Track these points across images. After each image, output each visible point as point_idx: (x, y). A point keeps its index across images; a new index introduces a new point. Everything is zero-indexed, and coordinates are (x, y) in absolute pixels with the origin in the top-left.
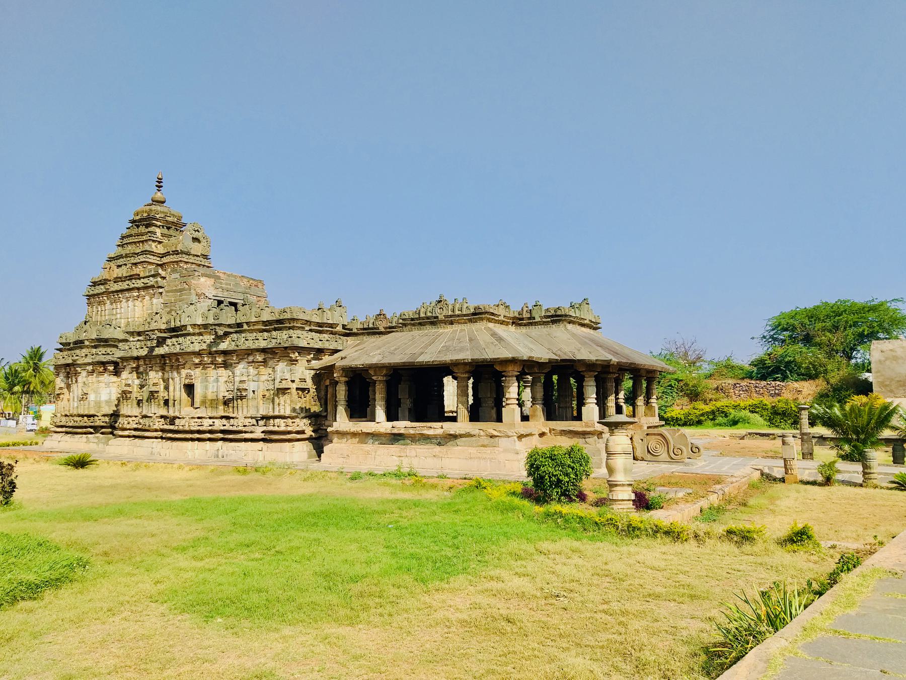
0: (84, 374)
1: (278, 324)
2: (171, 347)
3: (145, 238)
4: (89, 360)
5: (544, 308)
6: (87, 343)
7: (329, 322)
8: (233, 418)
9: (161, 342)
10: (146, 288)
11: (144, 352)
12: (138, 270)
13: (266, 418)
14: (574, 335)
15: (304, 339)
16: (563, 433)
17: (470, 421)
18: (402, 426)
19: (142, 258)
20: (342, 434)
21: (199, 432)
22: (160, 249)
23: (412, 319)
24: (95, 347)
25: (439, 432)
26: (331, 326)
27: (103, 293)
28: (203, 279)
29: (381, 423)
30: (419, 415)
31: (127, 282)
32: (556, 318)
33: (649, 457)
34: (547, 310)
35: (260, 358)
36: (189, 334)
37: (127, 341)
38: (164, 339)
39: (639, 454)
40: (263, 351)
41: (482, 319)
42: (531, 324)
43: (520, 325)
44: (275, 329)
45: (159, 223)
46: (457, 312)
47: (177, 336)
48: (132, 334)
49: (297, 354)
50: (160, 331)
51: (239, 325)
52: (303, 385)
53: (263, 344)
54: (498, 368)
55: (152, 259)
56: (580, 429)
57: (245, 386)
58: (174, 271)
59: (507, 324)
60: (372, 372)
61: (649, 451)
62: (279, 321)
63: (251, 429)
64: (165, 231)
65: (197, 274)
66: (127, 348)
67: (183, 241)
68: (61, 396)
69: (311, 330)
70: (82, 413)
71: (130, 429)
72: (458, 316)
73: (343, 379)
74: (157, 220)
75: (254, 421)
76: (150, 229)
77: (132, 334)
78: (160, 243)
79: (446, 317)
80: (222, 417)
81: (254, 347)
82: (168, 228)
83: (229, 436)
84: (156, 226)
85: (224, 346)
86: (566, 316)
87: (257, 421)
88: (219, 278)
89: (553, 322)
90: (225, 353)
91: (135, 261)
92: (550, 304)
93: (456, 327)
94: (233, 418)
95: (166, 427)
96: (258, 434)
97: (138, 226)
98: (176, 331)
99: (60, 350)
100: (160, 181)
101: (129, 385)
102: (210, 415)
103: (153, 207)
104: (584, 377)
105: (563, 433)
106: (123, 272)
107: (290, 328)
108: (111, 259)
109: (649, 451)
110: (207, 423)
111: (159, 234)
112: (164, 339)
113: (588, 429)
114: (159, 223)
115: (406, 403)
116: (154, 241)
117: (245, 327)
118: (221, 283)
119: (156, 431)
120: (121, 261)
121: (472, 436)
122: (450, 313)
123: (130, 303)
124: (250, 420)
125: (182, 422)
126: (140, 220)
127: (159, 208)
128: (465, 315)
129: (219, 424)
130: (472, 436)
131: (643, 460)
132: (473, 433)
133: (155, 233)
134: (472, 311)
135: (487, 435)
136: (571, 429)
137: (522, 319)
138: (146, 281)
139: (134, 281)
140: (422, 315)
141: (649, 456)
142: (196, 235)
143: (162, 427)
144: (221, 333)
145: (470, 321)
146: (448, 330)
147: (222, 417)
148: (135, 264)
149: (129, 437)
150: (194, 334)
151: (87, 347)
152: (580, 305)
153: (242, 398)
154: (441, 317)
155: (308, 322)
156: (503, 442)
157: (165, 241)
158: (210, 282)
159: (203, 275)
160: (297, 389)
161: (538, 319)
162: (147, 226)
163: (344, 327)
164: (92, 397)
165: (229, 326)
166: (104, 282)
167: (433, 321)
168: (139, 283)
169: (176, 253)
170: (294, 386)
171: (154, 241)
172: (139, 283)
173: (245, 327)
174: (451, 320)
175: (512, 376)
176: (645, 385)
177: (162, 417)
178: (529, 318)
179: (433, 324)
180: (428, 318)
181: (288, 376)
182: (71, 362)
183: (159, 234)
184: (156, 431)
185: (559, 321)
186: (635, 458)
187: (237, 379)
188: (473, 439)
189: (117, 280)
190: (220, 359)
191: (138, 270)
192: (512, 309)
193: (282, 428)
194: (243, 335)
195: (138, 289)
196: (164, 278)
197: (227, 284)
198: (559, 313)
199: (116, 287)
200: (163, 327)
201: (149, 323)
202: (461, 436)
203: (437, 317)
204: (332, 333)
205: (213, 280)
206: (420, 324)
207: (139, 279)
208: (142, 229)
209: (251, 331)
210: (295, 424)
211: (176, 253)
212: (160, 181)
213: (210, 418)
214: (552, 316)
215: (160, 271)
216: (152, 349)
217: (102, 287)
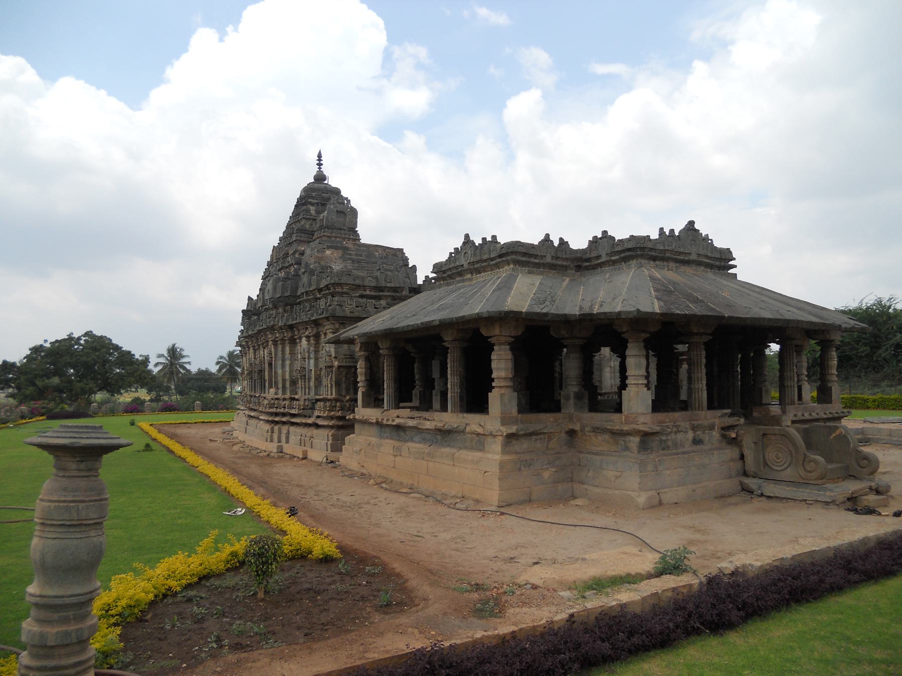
7: (388, 285)
26: (395, 289)
28: (328, 252)
43: (587, 268)
63: (307, 412)
69: (362, 296)
73: (362, 353)
84: (312, 204)
88: (347, 249)
104: (626, 341)
111: (313, 212)
113: (626, 428)
118: (350, 254)
133: (308, 211)
154: (466, 266)
158: (337, 254)
159: (328, 248)
161: (603, 259)
183: (313, 212)
185: (632, 258)
197: (357, 255)
205: (340, 252)
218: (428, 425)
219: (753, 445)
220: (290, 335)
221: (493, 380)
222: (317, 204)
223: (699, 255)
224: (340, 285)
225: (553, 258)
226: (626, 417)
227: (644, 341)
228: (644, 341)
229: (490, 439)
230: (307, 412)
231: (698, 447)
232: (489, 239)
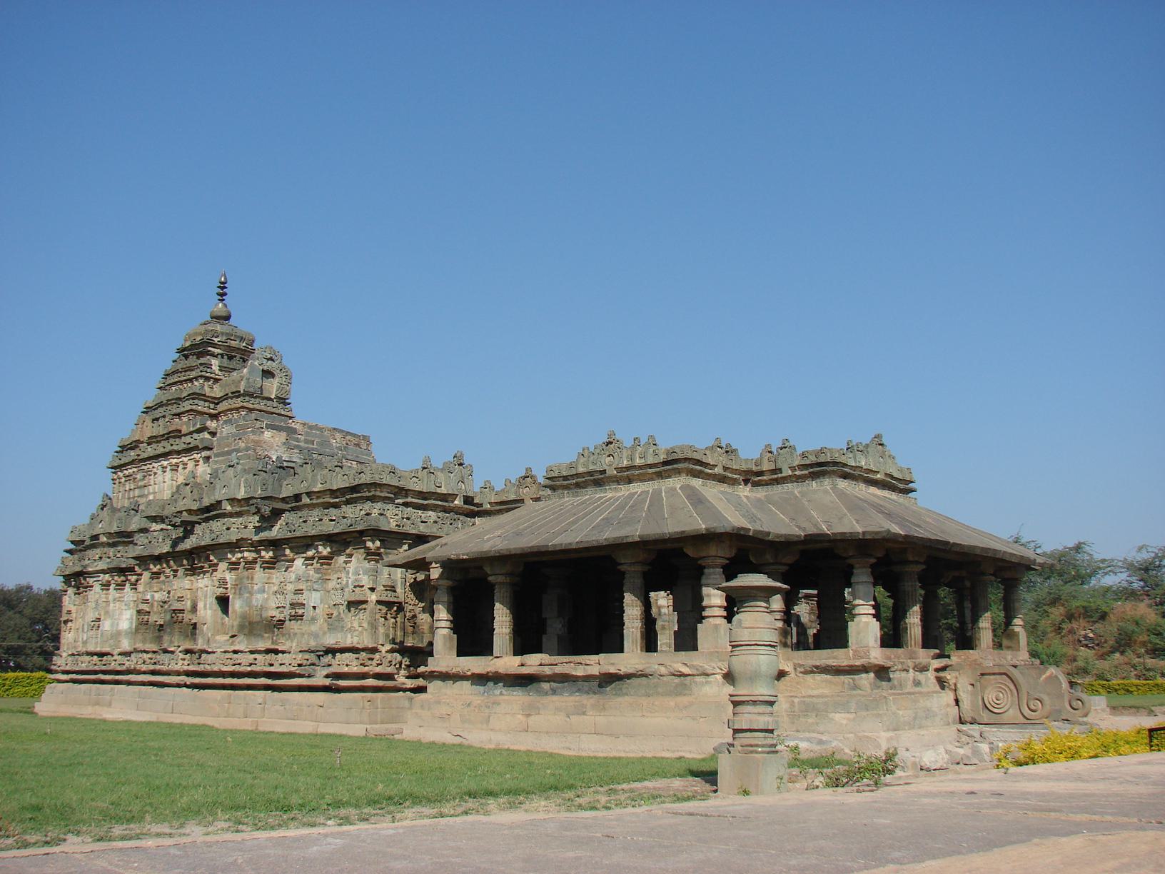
0: (97, 587)
1: (353, 494)
2: (202, 535)
3: (193, 374)
4: (102, 565)
5: (799, 451)
6: (103, 539)
7: (439, 490)
8: (283, 652)
9: (188, 528)
10: (189, 450)
11: (166, 549)
12: (184, 424)
13: (332, 651)
14: (842, 495)
15: (392, 517)
18: (533, 662)
19: (186, 406)
20: (445, 677)
21: (233, 675)
22: (217, 391)
23: (566, 478)
24: (113, 545)
25: (595, 670)
27: (132, 462)
28: (267, 434)
29: (505, 661)
30: (577, 645)
31: (164, 443)
32: (819, 468)
33: (985, 716)
34: (803, 455)
35: (325, 551)
36: (224, 515)
37: (144, 531)
38: (193, 524)
40: (329, 539)
41: (679, 472)
42: (777, 481)
44: (348, 502)
45: (217, 351)
46: (638, 461)
47: (207, 520)
48: (154, 519)
49: (378, 543)
50: (190, 512)
51: (297, 497)
52: (389, 597)
53: (329, 528)
54: (690, 551)
55: (202, 406)
57: (301, 598)
58: (228, 422)
59: (734, 482)
60: (488, 570)
62: (354, 489)
63: (310, 670)
64: (226, 362)
65: (258, 424)
66: (146, 541)
67: (245, 376)
68: (70, 624)
69: (406, 505)
70: (91, 648)
71: (144, 673)
72: (640, 467)
74: (215, 346)
75: (313, 658)
76: (202, 360)
77: (154, 519)
78: (217, 380)
79: (620, 470)
80: (268, 651)
81: (313, 533)
82: (230, 358)
83: (276, 682)
84: (213, 355)
85: (275, 533)
86: (835, 464)
87: (319, 656)
88: (294, 431)
89: (814, 476)
90: (275, 544)
91: (178, 411)
92: (808, 442)
93: (637, 488)
94: (283, 652)
95: (192, 668)
96: (319, 680)
97: (186, 357)
98: (211, 512)
99: (70, 552)
100: (223, 286)
101: (146, 601)
102: (251, 648)
103: (210, 327)
104: (852, 567)
106: (160, 429)
107: (368, 499)
108: (148, 410)
110: (246, 659)
111: (215, 368)
112: (193, 524)
114: (217, 351)
115: (555, 627)
116: (207, 379)
117: (306, 500)
118: (298, 440)
119: (178, 673)
120: (158, 413)
122: (625, 463)
123: (169, 474)
124: (307, 656)
125: (210, 658)
126: (193, 346)
127: (219, 327)
128: (651, 466)
129: (262, 663)
132: (648, 671)
133: (209, 366)
134: (662, 457)
137: (761, 473)
138: (188, 439)
139: (171, 441)
140: (581, 470)
142: (268, 365)
143: (186, 668)
144: (266, 510)
145: (660, 475)
146: (624, 490)
147: (268, 651)
148: (178, 415)
149: (143, 684)
150: (231, 515)
151: (103, 545)
152: (867, 446)
153: (297, 617)
154: (612, 472)
155: (401, 491)
157: (225, 378)
158: (281, 437)
159: (269, 427)
160: (379, 602)
161: (787, 472)
162: (200, 355)
163: (468, 500)
164: (106, 625)
165: (283, 500)
166: (135, 445)
167: (598, 479)
168: (179, 445)
169: (237, 394)
170: (373, 597)
171: (207, 379)
172: (179, 445)
173: (306, 500)
174: (628, 475)
175: (716, 566)
177: (187, 651)
178: (774, 471)
179: (598, 483)
180: (590, 473)
181: (366, 581)
182: (78, 569)
183: (215, 368)
184: (178, 673)
185: (823, 474)
187: (290, 587)
189: (153, 440)
190: (268, 555)
191: (184, 424)
192: (743, 454)
193: (355, 669)
194: (300, 514)
195: (178, 453)
196: (213, 434)
197: (306, 442)
198: (822, 459)
199: (150, 451)
200: (195, 507)
201: (176, 501)
202: (629, 676)
203: (604, 472)
204: (446, 510)
205: (284, 435)
206: (578, 485)
207: (180, 437)
208: (193, 361)
209: (311, 507)
210: (374, 662)
211: (237, 394)
212: (223, 286)
213: (252, 652)
214: (811, 466)
215: (209, 423)
216: (175, 543)
217: (132, 453)
218: (580, 672)
219: (970, 688)
220: (271, 554)
221: (704, 609)
222: (222, 355)
223: (886, 474)
224: (380, 485)
225: (726, 469)
226: (855, 651)
227: (872, 566)
228: (872, 566)
229: (702, 679)
230: (310, 670)
231: (917, 689)
232: (644, 440)
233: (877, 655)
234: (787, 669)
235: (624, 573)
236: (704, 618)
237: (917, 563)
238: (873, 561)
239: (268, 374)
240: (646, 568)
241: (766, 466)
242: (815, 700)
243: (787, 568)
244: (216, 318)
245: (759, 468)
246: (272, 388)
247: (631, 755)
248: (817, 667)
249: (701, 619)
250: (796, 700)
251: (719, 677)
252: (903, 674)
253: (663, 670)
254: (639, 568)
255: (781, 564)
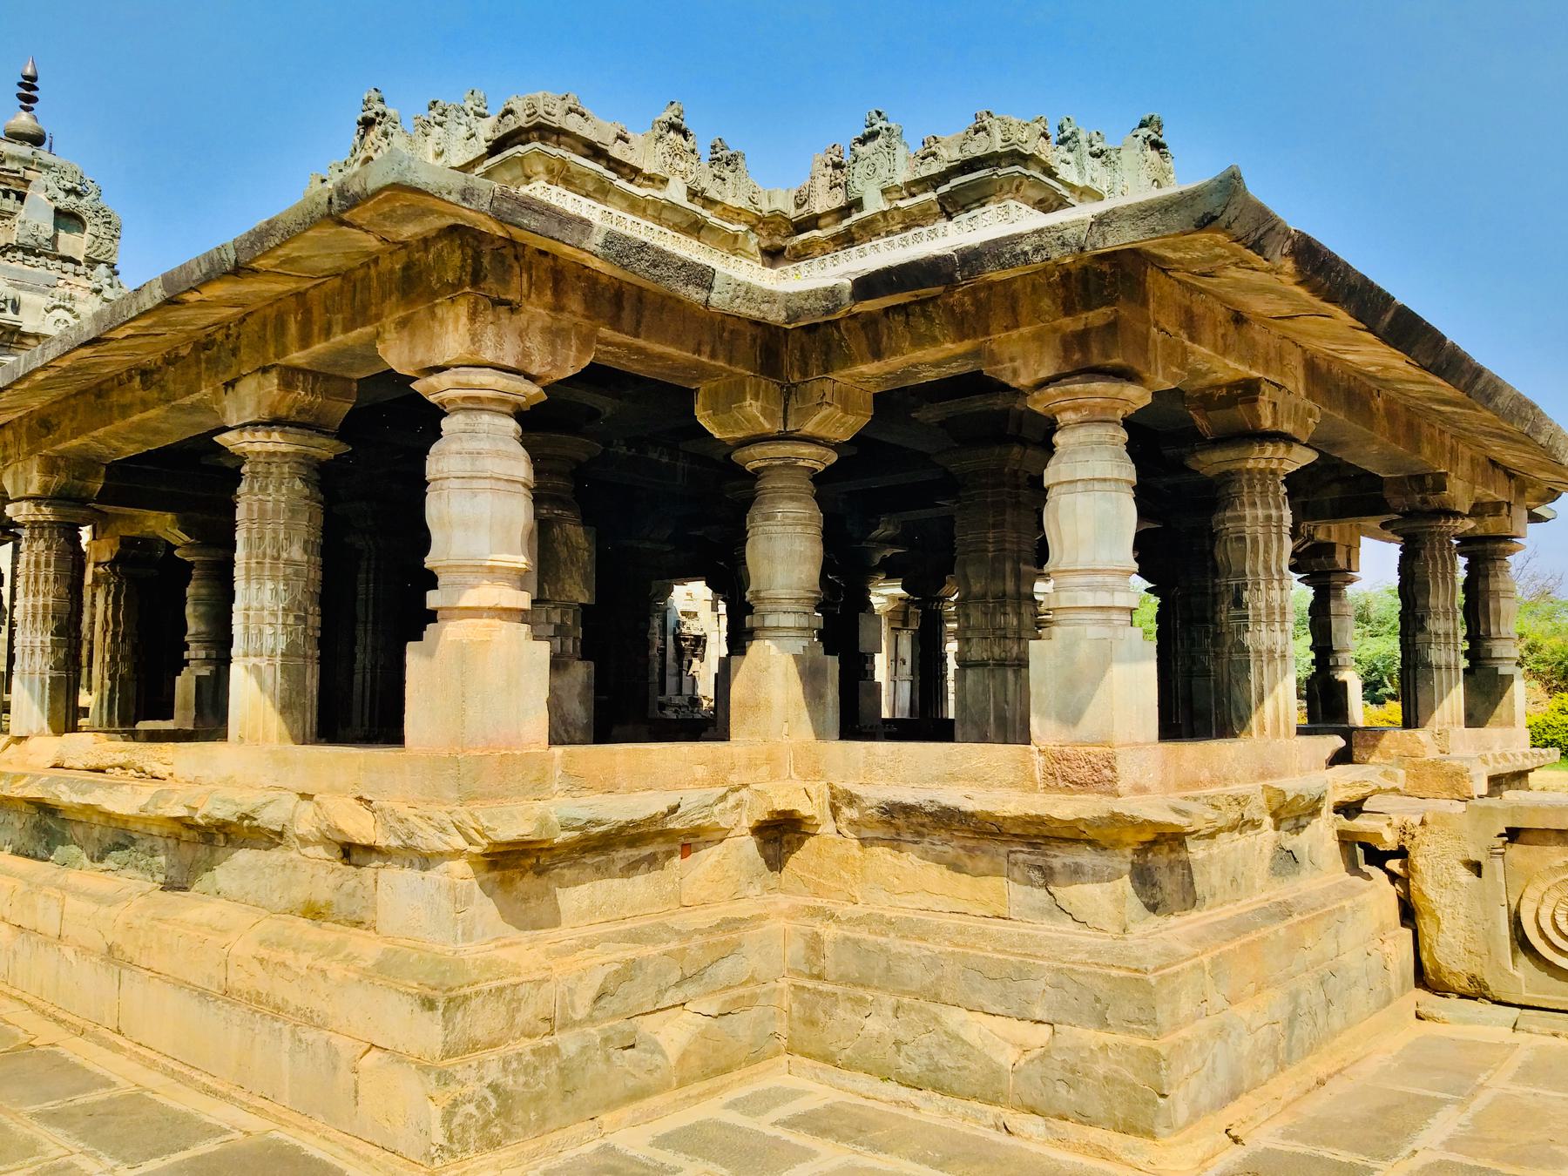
16: (903, 823)
17: (841, 738)
33: (1522, 978)
39: (1450, 947)
56: (1009, 803)
61: (1522, 943)
100: (29, 83)
105: (903, 823)
109: (1522, 943)
113: (1065, 808)
121: (273, 838)
130: (273, 838)
131: (1477, 992)
132: (269, 818)
135: (325, 841)
136: (953, 796)
137: (812, 222)
141: (1524, 969)
142: (66, 202)
156: (394, 886)
175: (475, 405)
176: (1462, 574)
186: (1422, 977)
188: (276, 855)
212: (29, 83)
214: (944, 177)
219: (1465, 876)
221: (431, 581)
225: (693, 194)
231: (1285, 890)
233: (1155, 778)
234: (804, 809)
235: (241, 459)
236: (432, 616)
237: (1289, 439)
238: (1136, 397)
239: (67, 219)
240: (325, 448)
241: (823, 202)
242: (895, 943)
243: (833, 457)
244: (16, 137)
245: (804, 211)
246: (74, 243)
247: (213, 1121)
248: (907, 810)
249: (418, 620)
250: (830, 932)
251: (460, 867)
252: (1241, 840)
253: (306, 822)
254: (275, 442)
255: (810, 440)
